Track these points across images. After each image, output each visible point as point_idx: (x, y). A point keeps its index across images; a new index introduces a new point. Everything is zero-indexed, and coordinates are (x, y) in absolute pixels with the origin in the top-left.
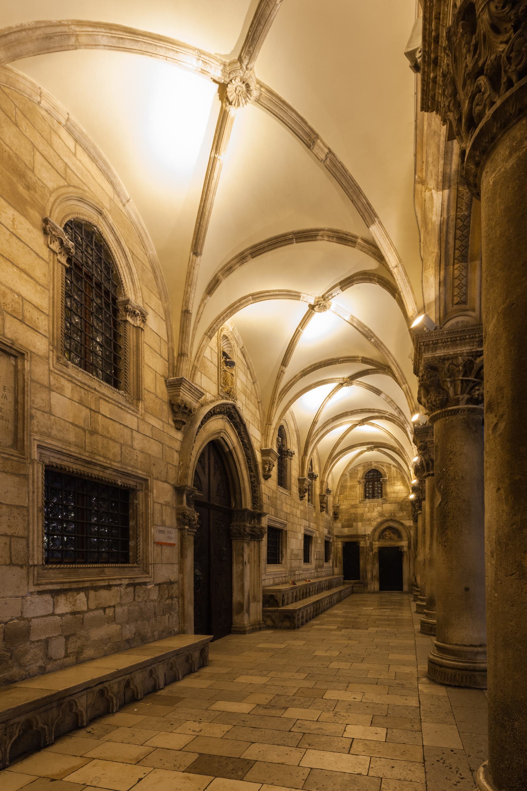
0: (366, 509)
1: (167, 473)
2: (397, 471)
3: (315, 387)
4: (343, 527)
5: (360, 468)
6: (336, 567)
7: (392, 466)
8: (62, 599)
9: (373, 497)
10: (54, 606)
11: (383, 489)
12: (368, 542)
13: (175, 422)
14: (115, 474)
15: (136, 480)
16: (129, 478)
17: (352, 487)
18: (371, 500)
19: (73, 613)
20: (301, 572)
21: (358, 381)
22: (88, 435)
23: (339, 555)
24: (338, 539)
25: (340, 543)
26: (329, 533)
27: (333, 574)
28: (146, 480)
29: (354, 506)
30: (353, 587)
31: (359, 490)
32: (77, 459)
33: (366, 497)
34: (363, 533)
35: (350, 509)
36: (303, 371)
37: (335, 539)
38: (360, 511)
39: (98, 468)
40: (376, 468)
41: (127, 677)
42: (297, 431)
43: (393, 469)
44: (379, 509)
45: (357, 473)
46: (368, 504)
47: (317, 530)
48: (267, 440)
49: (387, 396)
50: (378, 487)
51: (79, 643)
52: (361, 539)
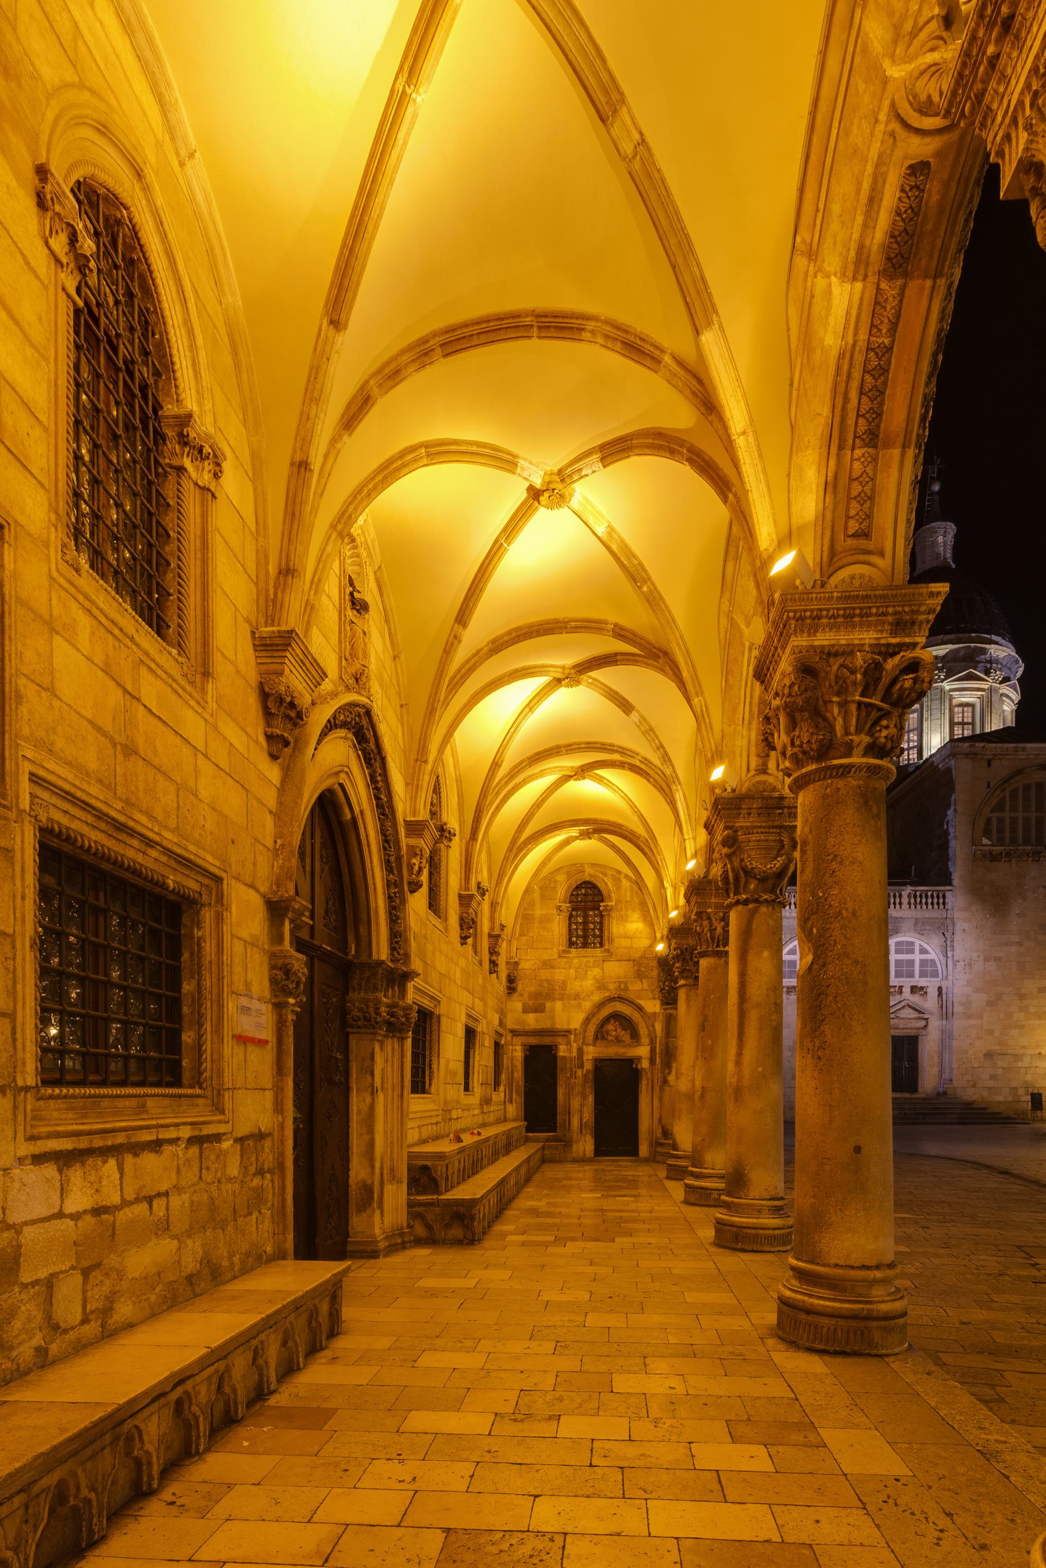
0: (572, 971)
1: (255, 864)
2: (632, 888)
3: (509, 682)
4: (525, 1011)
5: (561, 878)
6: (511, 1102)
7: (622, 877)
8: (76, 1175)
9: (585, 945)
10: (62, 1194)
11: (606, 927)
12: (575, 1046)
13: (269, 737)
14: (164, 859)
15: (200, 878)
16: (187, 872)
17: (545, 920)
18: (582, 951)
19: (98, 1211)
20: (460, 1113)
21: (590, 677)
22: (120, 758)
23: (516, 1075)
24: (515, 1039)
25: (519, 1048)
26: (501, 1023)
27: (505, 1120)
28: (218, 880)
29: (548, 964)
30: (543, 1148)
31: (558, 927)
32: (101, 815)
33: (571, 944)
34: (566, 1027)
35: (539, 969)
36: (494, 641)
37: (509, 1035)
38: (559, 975)
39: (135, 843)
40: (593, 880)
41: (221, 1365)
42: (459, 781)
43: (625, 883)
44: (597, 971)
45: (555, 889)
46: (575, 961)
47: (484, 1017)
48: (416, 798)
49: (643, 719)
50: (594, 923)
51: (106, 1288)
52: (560, 1040)
